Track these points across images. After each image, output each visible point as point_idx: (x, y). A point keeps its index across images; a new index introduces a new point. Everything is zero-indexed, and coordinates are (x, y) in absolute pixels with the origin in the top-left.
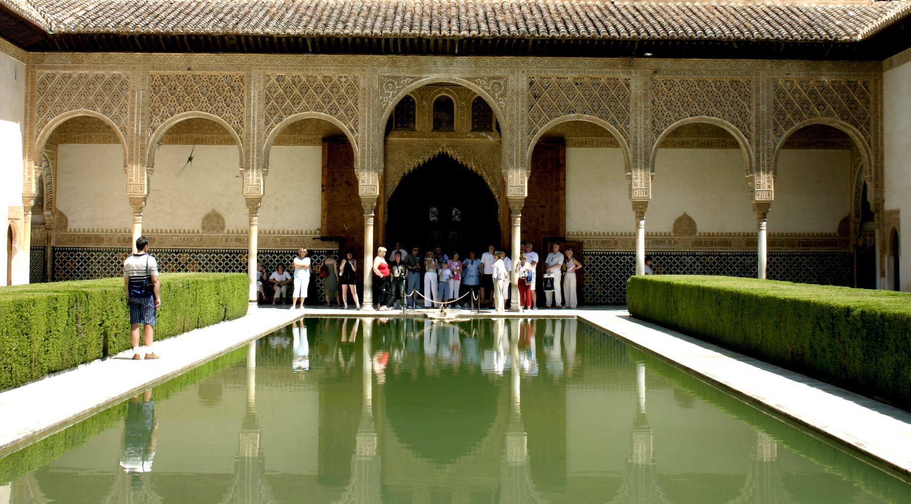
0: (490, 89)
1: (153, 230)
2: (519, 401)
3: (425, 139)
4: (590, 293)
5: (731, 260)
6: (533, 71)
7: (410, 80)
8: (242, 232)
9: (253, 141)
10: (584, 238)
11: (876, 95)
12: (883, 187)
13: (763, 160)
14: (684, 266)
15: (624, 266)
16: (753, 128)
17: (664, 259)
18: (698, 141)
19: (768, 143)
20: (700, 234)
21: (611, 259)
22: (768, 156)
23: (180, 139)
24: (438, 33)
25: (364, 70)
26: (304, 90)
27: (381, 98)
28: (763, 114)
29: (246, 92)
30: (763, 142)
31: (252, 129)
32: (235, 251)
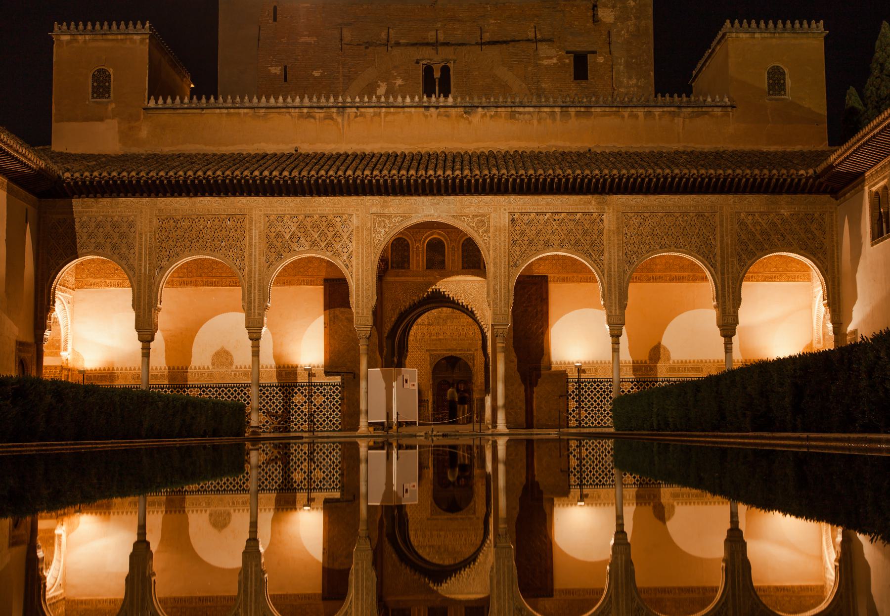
0: (474, 225)
7: (400, 219)
9: (255, 277)
10: (567, 366)
11: (832, 226)
12: (840, 312)
13: (728, 287)
15: (604, 392)
16: (718, 258)
18: (670, 276)
20: (674, 362)
21: (592, 385)
22: (733, 283)
24: (424, 173)
27: (374, 235)
28: (727, 244)
29: (247, 232)
30: (728, 270)
31: (253, 267)
32: (243, 385)
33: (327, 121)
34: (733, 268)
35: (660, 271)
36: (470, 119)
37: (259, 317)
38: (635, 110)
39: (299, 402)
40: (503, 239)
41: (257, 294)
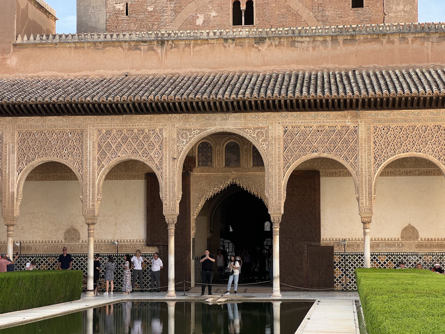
1: (30, 241)
3: (219, 173)
4: (340, 282)
6: (286, 122)
7: (198, 131)
9: (90, 177)
14: (410, 263)
17: (395, 258)
20: (421, 239)
21: (354, 258)
23: (49, 176)
25: (165, 125)
26: (124, 141)
31: (88, 169)
33: (150, 52)
35: (410, 167)
36: (260, 48)
38: (392, 38)
40: (277, 146)
41: (91, 191)
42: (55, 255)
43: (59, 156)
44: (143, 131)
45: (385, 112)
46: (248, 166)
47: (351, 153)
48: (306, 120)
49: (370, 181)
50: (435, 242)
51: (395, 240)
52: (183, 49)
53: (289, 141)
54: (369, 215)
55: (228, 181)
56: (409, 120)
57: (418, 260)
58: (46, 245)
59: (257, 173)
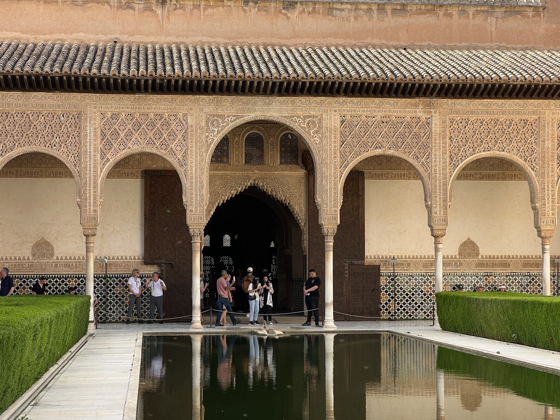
2: (333, 409)
3: (238, 172)
4: (387, 310)
5: (510, 279)
6: (344, 111)
7: (233, 118)
8: (70, 258)
9: (90, 174)
19: (552, 175)
20: (482, 257)
23: (10, 172)
25: (191, 109)
27: (207, 134)
28: (548, 149)
30: (548, 174)
31: (88, 163)
32: (64, 276)
33: (147, 13)
34: (552, 172)
36: (289, 15)
37: (94, 214)
39: (120, 293)
40: (333, 140)
41: (92, 192)
42: (19, 276)
43: (48, 145)
44: (161, 116)
45: (464, 102)
46: (274, 163)
47: (422, 151)
48: (368, 108)
49: (445, 185)
50: (498, 260)
51: (452, 258)
52: (191, 10)
53: (348, 134)
54: (443, 227)
55: (248, 182)
56: (491, 112)
57: (477, 282)
58: (7, 263)
59: (286, 173)
